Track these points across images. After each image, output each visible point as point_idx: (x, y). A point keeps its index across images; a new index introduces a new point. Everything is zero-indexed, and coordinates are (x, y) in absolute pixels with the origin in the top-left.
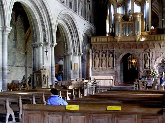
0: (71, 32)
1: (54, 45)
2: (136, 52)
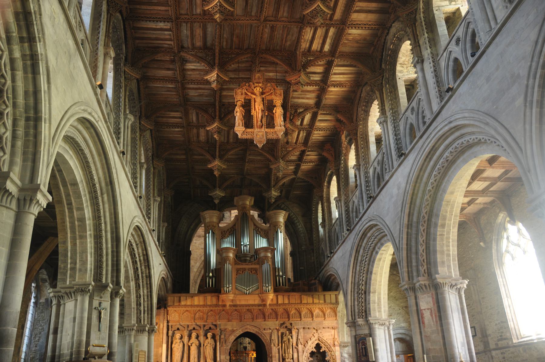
0: (138, 275)
1: (121, 291)
2: (264, 329)
